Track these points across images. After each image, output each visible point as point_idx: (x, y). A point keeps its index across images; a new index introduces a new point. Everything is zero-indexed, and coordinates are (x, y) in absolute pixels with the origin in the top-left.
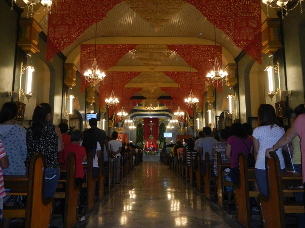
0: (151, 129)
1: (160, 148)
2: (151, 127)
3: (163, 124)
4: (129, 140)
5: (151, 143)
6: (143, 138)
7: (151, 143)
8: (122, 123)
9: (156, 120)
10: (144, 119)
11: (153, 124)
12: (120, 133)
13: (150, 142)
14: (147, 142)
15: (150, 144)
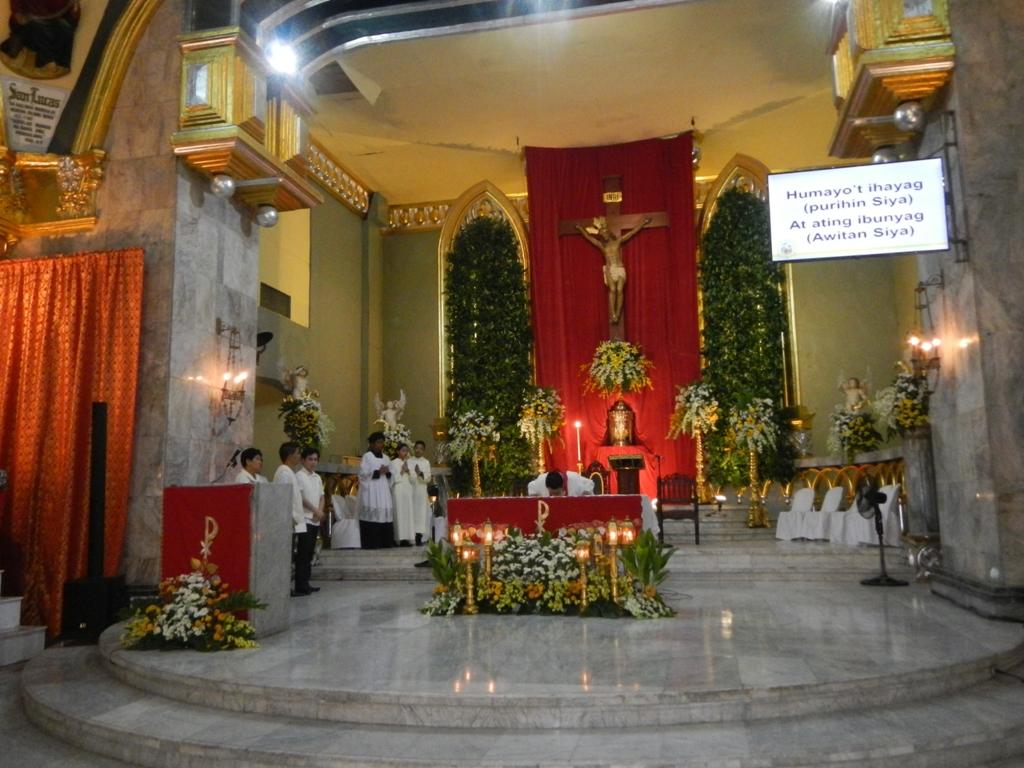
0: (616, 272)
1: (716, 476)
2: (612, 250)
3: (745, 196)
4: (152, 338)
5: (620, 430)
6: (523, 371)
7: (620, 430)
8: (70, 81)
9: (661, 165)
10: (541, 164)
11: (634, 222)
12: (46, 240)
13: (610, 423)
14: (576, 411)
15: (609, 441)
